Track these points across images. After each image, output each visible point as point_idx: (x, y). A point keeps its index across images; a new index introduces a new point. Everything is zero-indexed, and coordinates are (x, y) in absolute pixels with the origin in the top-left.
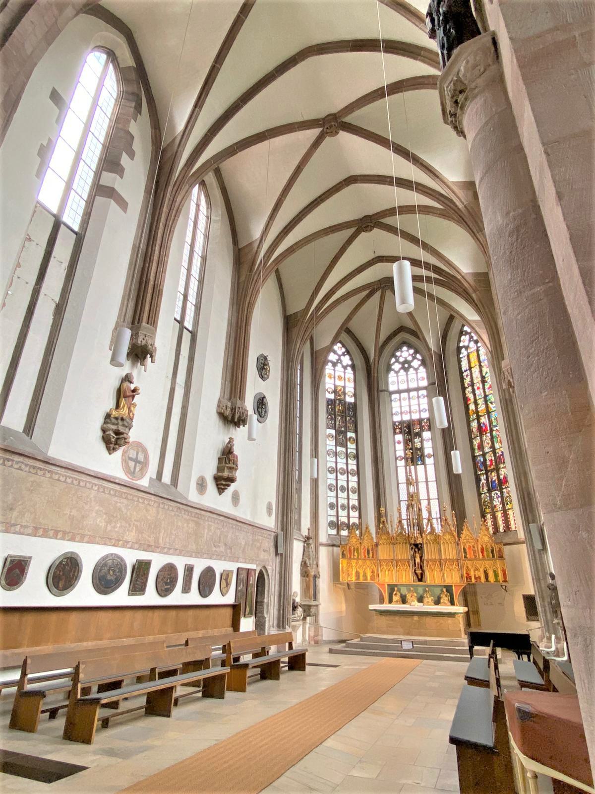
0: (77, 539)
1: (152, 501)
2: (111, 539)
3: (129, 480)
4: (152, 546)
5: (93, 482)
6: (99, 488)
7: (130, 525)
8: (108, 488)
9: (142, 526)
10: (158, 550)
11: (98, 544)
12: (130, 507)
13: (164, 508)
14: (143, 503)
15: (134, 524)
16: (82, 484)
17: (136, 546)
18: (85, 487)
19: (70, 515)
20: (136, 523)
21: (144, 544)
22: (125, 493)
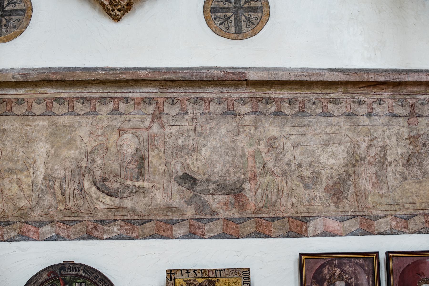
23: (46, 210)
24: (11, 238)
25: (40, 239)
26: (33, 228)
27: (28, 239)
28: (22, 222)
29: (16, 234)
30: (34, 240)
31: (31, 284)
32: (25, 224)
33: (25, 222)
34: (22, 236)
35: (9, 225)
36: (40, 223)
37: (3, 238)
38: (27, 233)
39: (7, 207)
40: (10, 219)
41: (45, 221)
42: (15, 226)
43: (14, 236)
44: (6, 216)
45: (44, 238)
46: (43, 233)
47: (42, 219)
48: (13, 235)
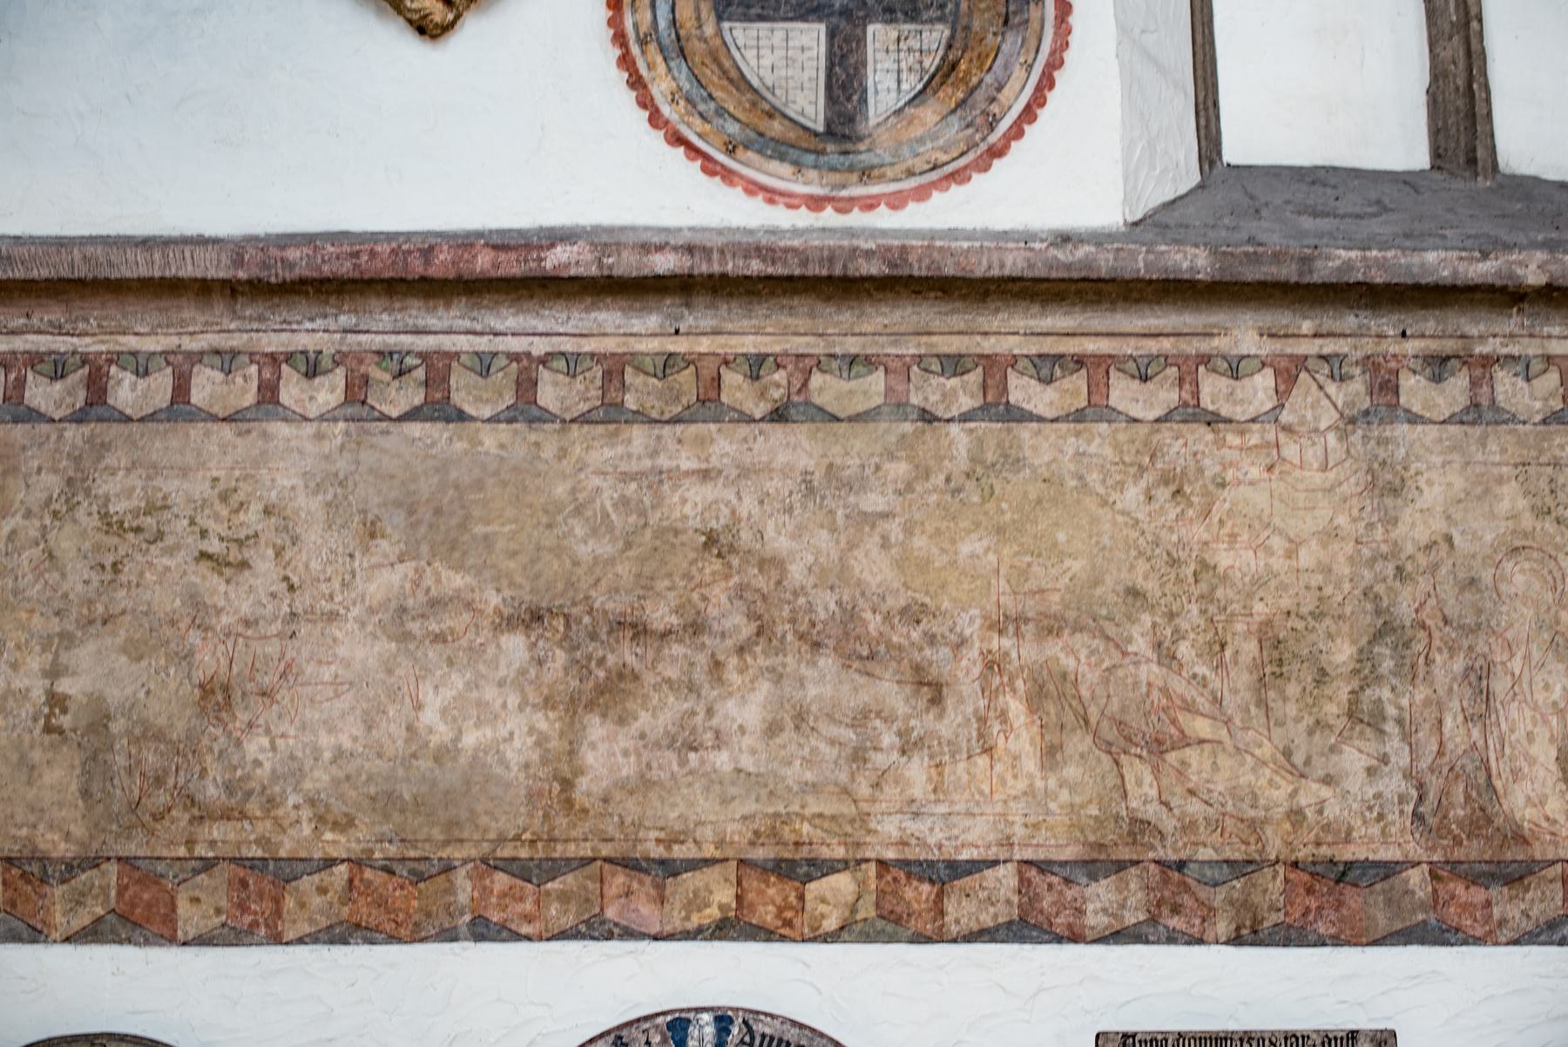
0: (190, 917)
1: (1235, 369)
2: (671, 868)
3: (802, 218)
4: (1389, 870)
5: (272, 342)
6: (357, 390)
7: (933, 691)
8: (484, 364)
9: (1151, 672)
10: (1509, 907)
11: (483, 930)
12: (873, 502)
13: (1476, 413)
14: (1093, 411)
15: (993, 664)
16: (126, 392)
17: (1099, 898)
18: (180, 406)
19: (57, 701)
20: (1024, 651)
21: (1243, 868)
22: (756, 365)
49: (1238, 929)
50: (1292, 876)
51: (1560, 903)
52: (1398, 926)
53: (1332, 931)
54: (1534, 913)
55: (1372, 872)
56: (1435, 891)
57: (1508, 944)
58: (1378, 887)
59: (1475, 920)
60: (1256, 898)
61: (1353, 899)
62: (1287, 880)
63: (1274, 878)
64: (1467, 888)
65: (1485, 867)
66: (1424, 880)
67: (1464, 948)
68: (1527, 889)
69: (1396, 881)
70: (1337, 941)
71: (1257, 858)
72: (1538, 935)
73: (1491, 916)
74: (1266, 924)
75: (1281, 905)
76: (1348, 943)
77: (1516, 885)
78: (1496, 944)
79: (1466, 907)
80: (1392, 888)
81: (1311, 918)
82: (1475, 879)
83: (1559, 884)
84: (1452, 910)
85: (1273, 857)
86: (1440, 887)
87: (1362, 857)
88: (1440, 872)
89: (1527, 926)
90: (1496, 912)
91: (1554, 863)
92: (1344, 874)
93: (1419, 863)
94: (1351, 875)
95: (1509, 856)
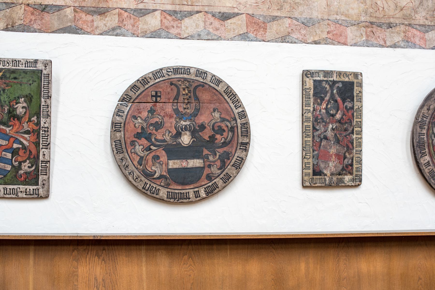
4: (59, 8)
10: (99, 22)
23: (432, 13)
24: (395, 44)
25: (427, 47)
26: (418, 33)
27: (414, 46)
28: (406, 25)
29: (401, 39)
30: (421, 48)
31: (432, 100)
32: (410, 28)
33: (410, 25)
34: (407, 42)
35: (391, 28)
36: (425, 28)
37: (385, 43)
38: (412, 39)
39: (387, 5)
40: (392, 20)
41: (431, 26)
42: (398, 29)
43: (398, 42)
44: (386, 17)
45: (432, 46)
46: (430, 39)
47: (428, 23)
48: (397, 40)
49: (7, 25)
50: (27, 9)
51: (117, 22)
52: (61, 27)
53: (39, 27)
54: (108, 25)
55: (54, 8)
56: (75, 16)
57: (98, 35)
58: (55, 13)
59: (88, 26)
60: (14, 15)
61: (47, 17)
62: (25, 10)
63: (21, 9)
64: (86, 15)
65: (92, 9)
66: (71, 12)
67: (83, 35)
68: (106, 17)
69: (62, 12)
70: (40, 31)
71: (15, 2)
72: (109, 32)
73: (93, 25)
74: (17, 24)
75: (22, 18)
76: (44, 32)
77: (103, 15)
78: (94, 34)
79: (85, 22)
80: (60, 14)
81: (32, 23)
82: (88, 13)
83: (117, 16)
84: (80, 22)
85: (20, 2)
86: (76, 14)
87: (51, 4)
88: (77, 10)
89: (106, 29)
90: (95, 24)
91: (116, 9)
92: (44, 9)
93: (70, 6)
94: (47, 9)
95: (101, 5)
